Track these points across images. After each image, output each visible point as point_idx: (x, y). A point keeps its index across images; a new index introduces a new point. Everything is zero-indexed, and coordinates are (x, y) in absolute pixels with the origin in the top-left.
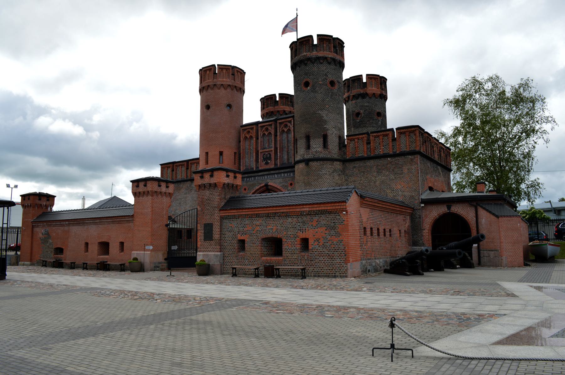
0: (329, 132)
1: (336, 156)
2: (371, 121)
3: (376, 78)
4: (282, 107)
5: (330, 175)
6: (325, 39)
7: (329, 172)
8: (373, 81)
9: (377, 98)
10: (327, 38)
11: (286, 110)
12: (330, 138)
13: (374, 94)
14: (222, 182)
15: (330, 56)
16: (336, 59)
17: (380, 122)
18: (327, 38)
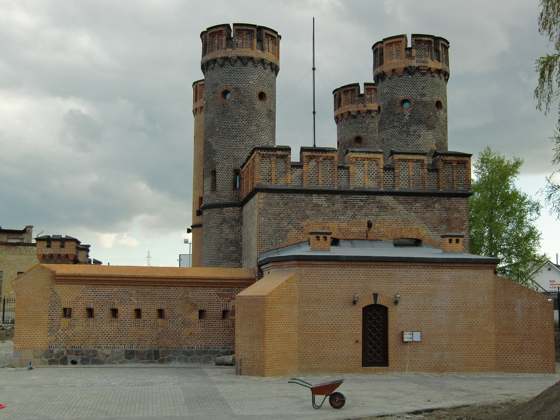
0: (218, 167)
1: (226, 200)
2: (391, 118)
3: (398, 42)
4: (347, 106)
5: (217, 227)
6: (215, 33)
7: (216, 224)
8: (394, 49)
9: (400, 76)
10: (218, 29)
11: (351, 110)
12: (218, 174)
13: (394, 70)
14: (40, 254)
15: (219, 56)
16: (230, 56)
17: (407, 118)
18: (218, 29)
